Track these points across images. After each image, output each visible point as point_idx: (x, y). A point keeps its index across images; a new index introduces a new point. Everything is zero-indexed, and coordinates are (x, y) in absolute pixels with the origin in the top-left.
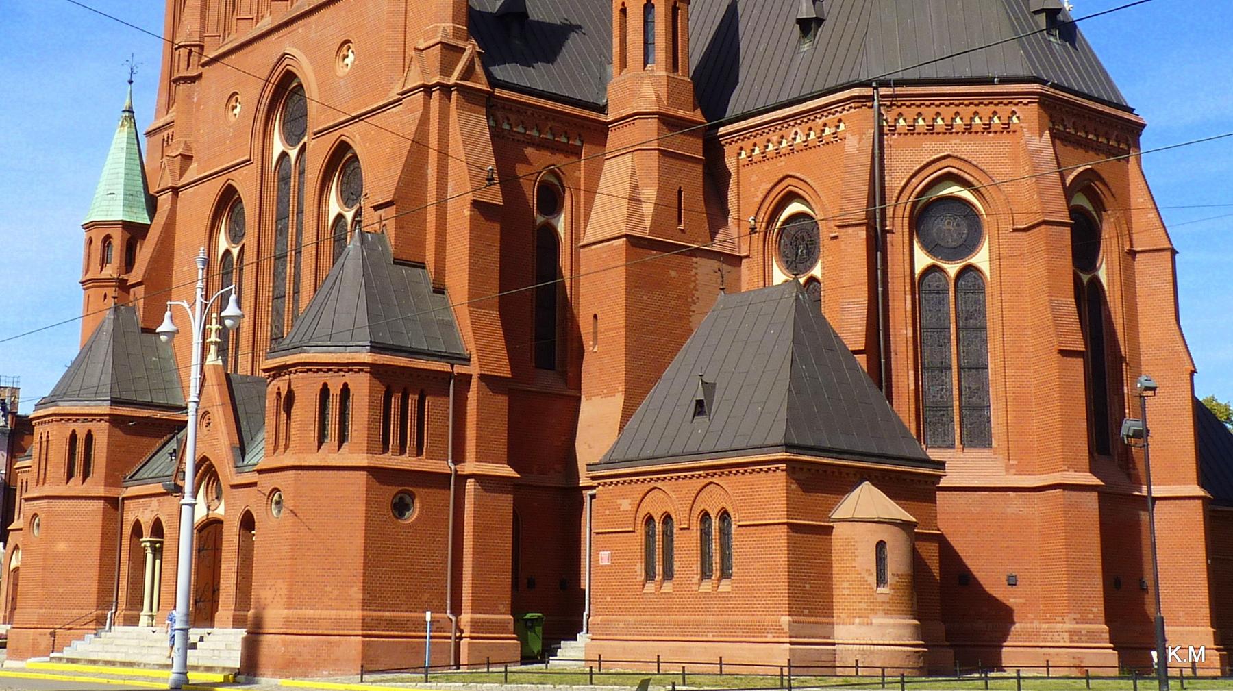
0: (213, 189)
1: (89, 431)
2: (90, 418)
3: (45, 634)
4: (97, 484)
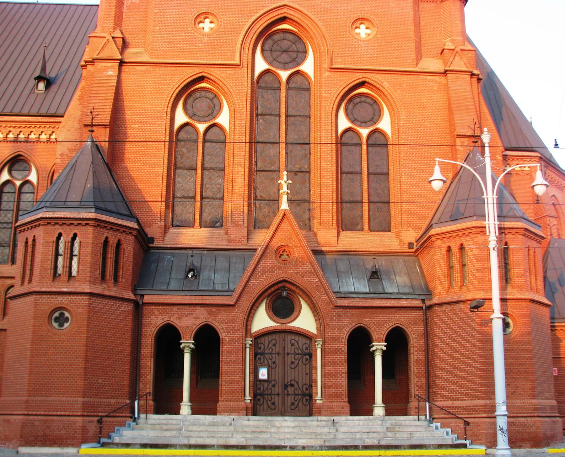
0: (189, 74)
1: (119, 241)
2: (122, 229)
3: (93, 422)
4: (125, 289)
